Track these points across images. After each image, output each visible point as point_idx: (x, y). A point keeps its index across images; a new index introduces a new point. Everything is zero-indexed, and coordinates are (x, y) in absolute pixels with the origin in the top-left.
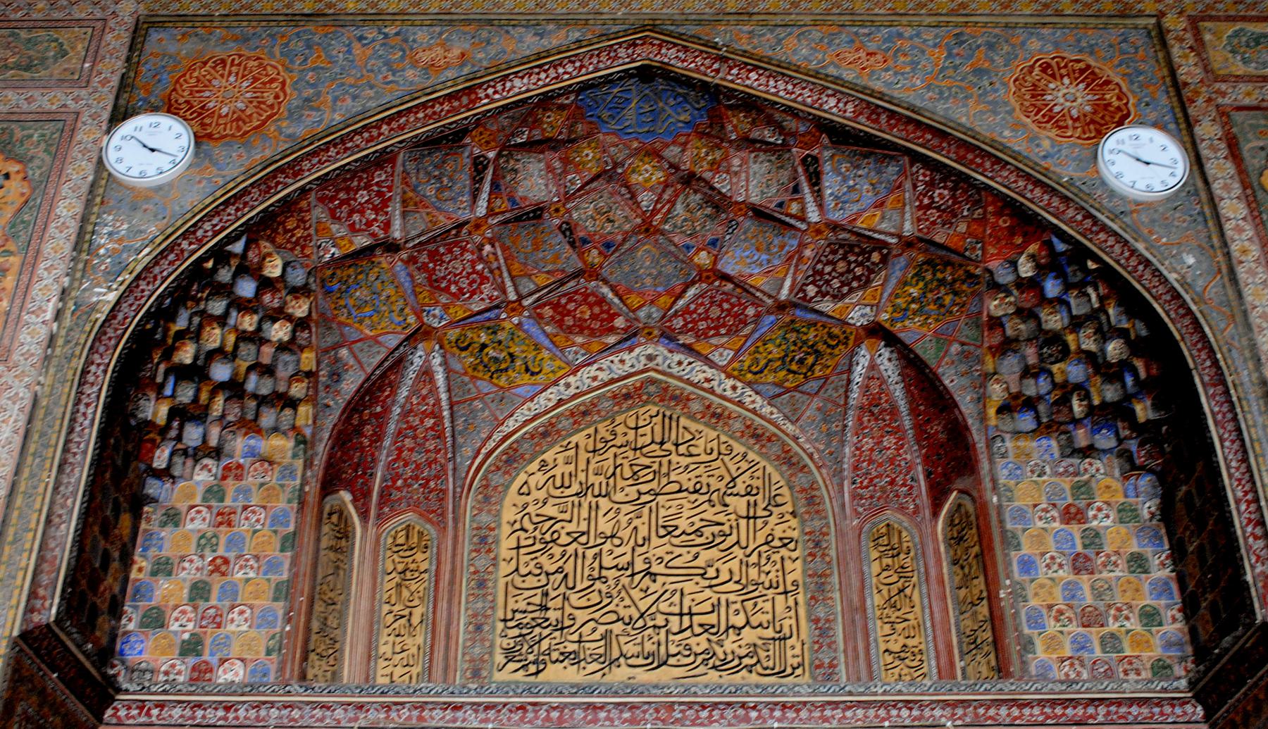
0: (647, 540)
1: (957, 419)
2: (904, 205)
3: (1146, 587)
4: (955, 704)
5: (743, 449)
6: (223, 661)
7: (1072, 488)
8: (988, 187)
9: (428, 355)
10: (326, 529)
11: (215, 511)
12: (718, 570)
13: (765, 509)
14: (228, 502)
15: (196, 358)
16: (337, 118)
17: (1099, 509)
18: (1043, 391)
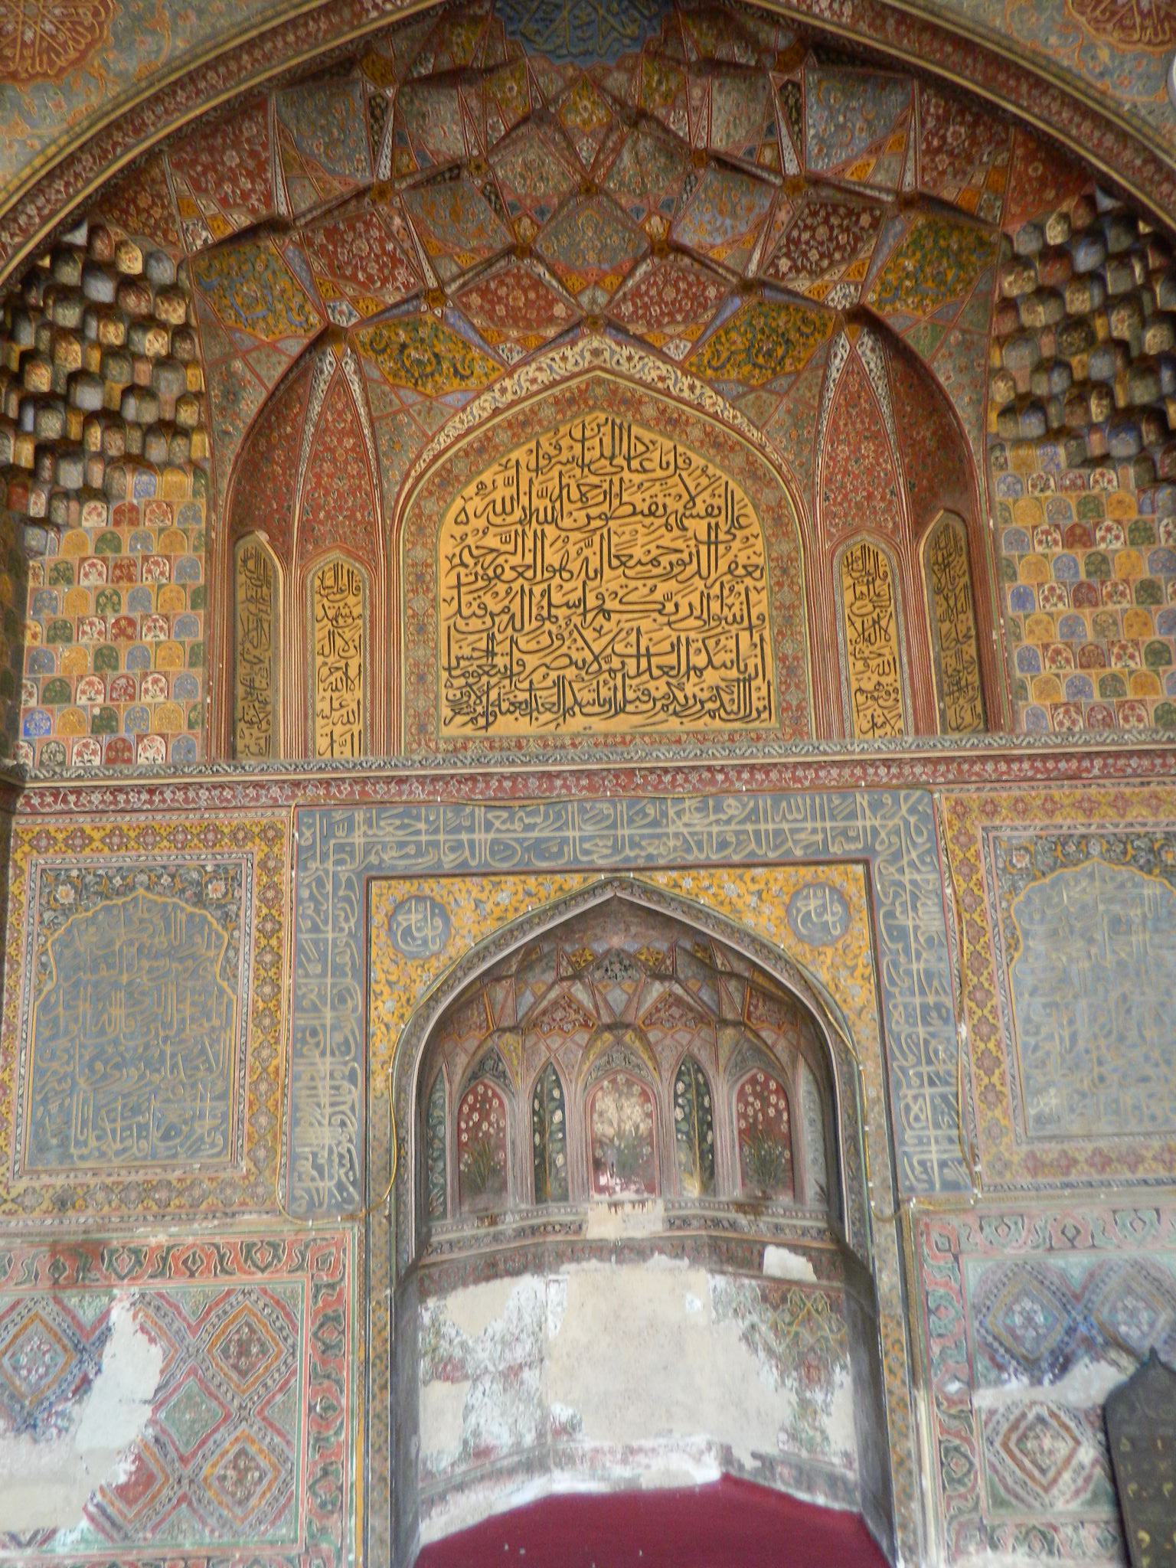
0: (599, 572)
1: (950, 425)
2: (907, 150)
3: (1156, 620)
4: (937, 761)
5: (702, 462)
6: (140, 738)
7: (1079, 504)
8: (1019, 122)
9: (338, 360)
10: (241, 578)
11: (111, 564)
12: (676, 605)
13: (728, 532)
14: (126, 552)
15: (54, 381)
16: (181, 45)
17: (1109, 529)
18: (1057, 389)
